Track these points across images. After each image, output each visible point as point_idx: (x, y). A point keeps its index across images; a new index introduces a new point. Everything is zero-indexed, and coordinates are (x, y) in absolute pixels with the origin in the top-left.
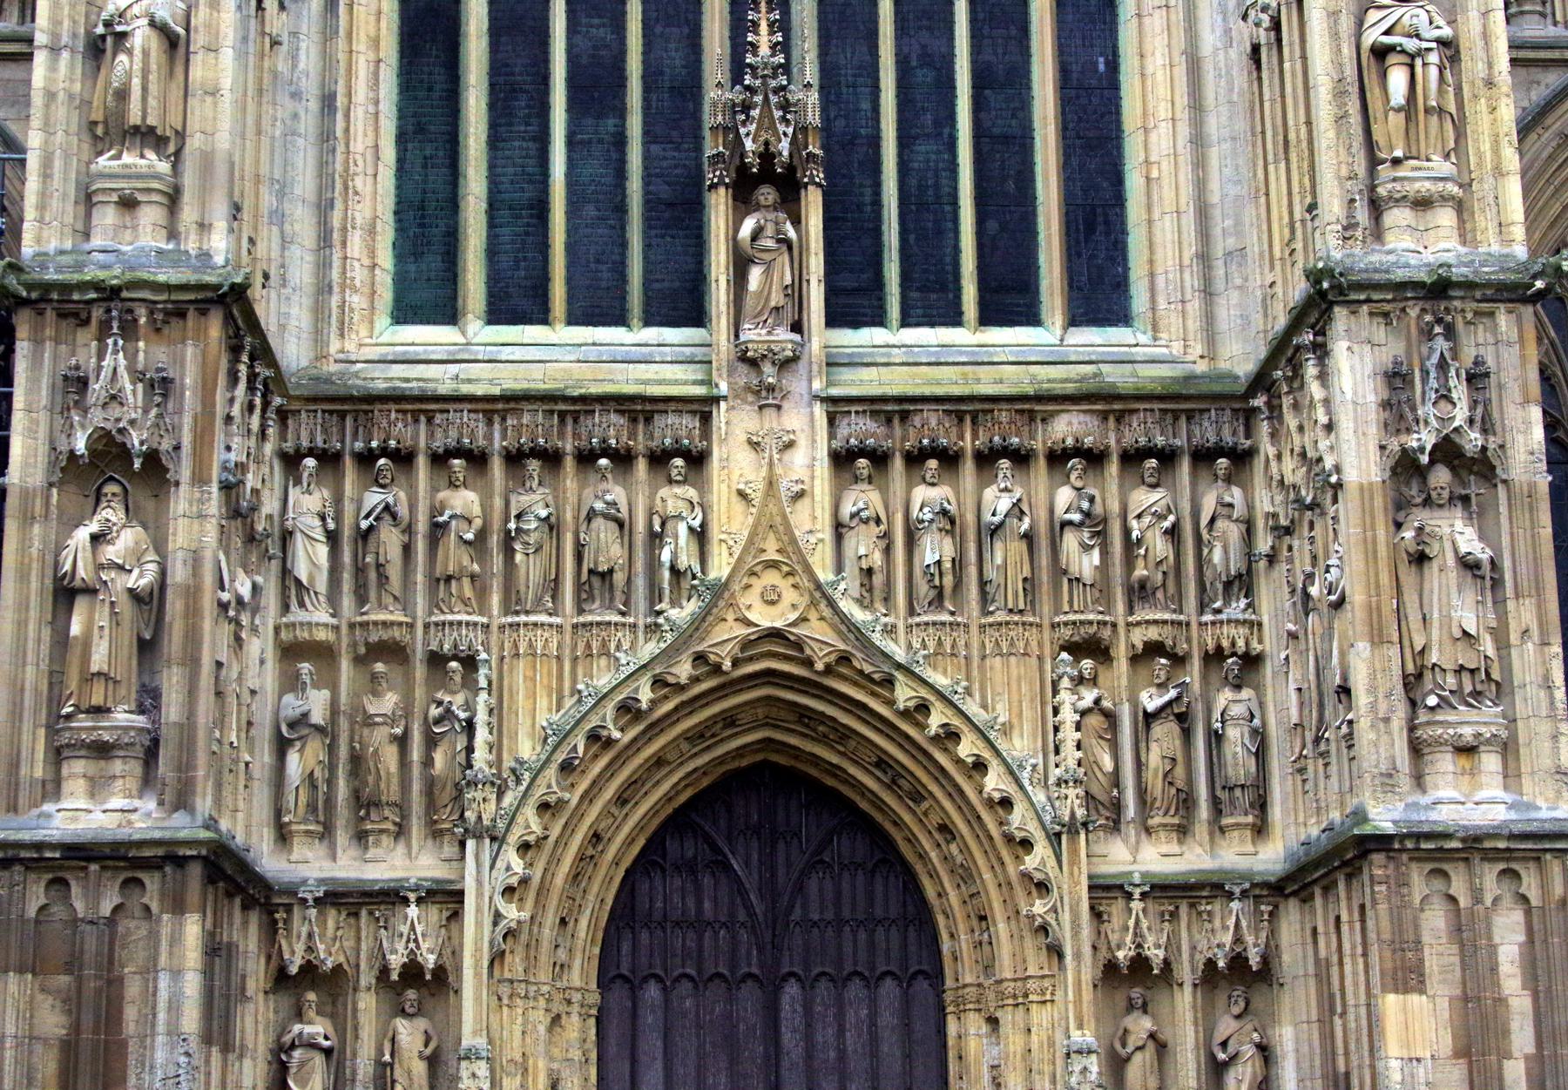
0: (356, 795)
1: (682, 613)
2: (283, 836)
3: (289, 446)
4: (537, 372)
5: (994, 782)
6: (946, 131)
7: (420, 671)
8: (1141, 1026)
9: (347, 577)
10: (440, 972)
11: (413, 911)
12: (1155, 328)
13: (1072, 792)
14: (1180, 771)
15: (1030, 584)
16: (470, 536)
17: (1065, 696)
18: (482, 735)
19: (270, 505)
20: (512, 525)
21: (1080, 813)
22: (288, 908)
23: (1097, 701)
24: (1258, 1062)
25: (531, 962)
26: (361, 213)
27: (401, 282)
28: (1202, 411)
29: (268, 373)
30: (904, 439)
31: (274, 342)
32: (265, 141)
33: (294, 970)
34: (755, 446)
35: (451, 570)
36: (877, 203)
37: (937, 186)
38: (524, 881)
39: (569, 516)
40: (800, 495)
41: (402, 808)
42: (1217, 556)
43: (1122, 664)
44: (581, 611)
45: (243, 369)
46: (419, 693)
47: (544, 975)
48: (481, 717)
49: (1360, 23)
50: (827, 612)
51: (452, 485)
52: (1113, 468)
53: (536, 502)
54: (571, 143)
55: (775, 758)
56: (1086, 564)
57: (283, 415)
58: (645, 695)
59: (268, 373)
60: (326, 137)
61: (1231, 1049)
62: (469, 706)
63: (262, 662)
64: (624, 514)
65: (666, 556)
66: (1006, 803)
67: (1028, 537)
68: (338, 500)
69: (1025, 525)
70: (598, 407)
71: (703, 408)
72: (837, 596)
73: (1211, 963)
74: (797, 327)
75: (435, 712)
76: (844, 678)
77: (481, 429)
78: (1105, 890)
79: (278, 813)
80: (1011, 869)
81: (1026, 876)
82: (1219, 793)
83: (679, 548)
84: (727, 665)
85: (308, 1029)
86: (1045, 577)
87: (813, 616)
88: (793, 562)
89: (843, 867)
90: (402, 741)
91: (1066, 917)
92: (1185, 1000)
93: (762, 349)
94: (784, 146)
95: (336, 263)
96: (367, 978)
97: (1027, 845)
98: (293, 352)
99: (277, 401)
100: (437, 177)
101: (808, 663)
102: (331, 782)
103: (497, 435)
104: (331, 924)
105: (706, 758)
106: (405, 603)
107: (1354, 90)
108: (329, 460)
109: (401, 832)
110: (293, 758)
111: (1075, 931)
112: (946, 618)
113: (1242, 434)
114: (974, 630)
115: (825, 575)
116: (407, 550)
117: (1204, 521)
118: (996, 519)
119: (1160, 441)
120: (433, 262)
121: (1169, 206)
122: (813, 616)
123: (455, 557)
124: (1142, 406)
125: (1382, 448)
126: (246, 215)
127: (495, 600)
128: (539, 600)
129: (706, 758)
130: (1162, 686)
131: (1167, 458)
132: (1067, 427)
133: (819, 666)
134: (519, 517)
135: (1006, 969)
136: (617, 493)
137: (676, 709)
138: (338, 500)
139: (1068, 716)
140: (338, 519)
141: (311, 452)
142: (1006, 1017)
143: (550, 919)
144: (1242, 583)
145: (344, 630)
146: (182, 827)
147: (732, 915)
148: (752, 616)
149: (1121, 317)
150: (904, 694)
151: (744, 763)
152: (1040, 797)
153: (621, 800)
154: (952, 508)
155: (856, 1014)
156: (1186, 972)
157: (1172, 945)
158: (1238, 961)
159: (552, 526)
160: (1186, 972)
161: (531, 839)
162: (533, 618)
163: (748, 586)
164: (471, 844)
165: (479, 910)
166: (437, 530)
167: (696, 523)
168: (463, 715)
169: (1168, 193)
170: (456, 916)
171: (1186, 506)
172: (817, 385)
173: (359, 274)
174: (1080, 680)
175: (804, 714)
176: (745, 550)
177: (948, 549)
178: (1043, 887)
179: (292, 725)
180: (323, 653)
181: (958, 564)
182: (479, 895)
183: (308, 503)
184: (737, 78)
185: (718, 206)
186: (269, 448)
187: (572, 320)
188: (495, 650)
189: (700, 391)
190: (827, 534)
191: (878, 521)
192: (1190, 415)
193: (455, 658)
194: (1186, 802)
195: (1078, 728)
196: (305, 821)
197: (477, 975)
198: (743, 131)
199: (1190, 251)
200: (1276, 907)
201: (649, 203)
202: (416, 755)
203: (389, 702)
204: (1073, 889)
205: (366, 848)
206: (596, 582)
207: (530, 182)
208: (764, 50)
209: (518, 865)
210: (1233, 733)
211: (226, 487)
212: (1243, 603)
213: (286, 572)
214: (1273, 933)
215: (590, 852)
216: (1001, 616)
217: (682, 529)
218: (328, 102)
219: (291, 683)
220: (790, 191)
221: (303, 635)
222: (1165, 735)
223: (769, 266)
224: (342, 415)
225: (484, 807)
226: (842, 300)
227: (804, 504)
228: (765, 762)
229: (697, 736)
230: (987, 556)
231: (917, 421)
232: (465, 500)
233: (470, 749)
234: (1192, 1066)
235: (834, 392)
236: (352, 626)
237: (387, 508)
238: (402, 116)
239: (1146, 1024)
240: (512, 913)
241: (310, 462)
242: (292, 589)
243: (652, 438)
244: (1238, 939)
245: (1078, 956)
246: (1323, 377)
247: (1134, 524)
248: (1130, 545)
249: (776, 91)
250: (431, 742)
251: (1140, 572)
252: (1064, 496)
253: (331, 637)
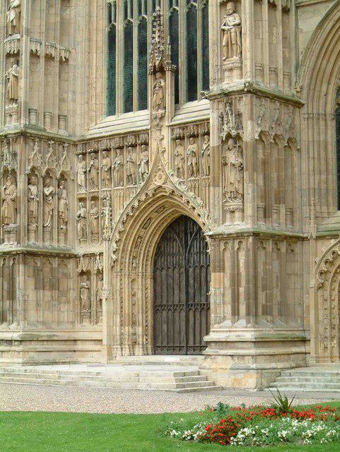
163: (155, 176)
240: (114, 257)
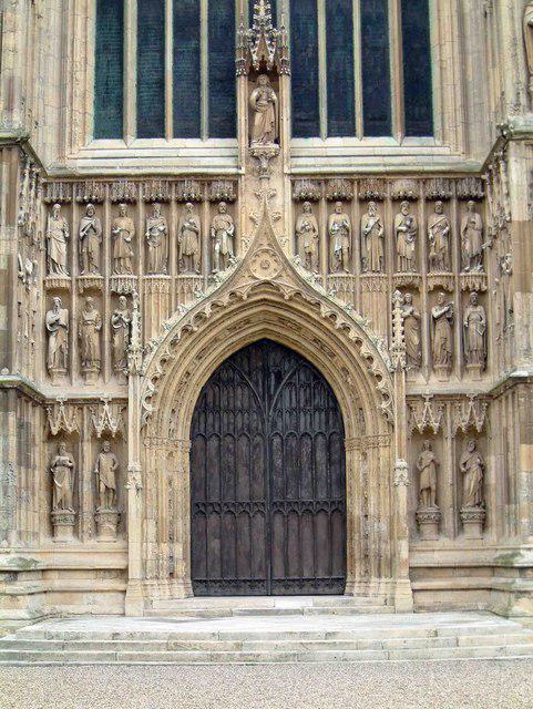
0: (81, 357)
1: (224, 275)
2: (49, 373)
3: (48, 199)
4: (160, 162)
5: (365, 350)
6: (333, 68)
7: (108, 300)
8: (428, 456)
9: (75, 258)
10: (119, 434)
11: (106, 407)
12: (443, 138)
13: (399, 354)
14: (448, 344)
15: (383, 259)
16: (129, 239)
17: (397, 311)
18: (135, 330)
19: (40, 227)
20: (148, 234)
21: (403, 363)
22: (53, 406)
23: (411, 313)
24: (479, 471)
25: (159, 430)
26: (79, 90)
27: (98, 119)
28: (462, 179)
29: (38, 170)
30: (327, 192)
31: (39, 156)
32: (36, 62)
33: (55, 432)
34: (258, 196)
35: (120, 255)
36: (316, 79)
37: (344, 71)
38: (155, 394)
39: (174, 229)
40: (278, 219)
41: (102, 362)
42: (468, 246)
43: (424, 295)
44: (179, 273)
45: (27, 172)
46: (107, 310)
47: (165, 434)
48: (134, 323)
49: (524, 11)
50: (290, 272)
51: (121, 216)
52: (422, 205)
53: (158, 223)
54: (176, 53)
55: (268, 337)
56: (407, 248)
57: (45, 185)
58: (208, 311)
59: (38, 170)
60: (63, 57)
61: (467, 467)
62: (129, 316)
63: (38, 297)
64: (198, 228)
65: (217, 247)
66: (370, 359)
67: (383, 238)
68: (70, 222)
69: (381, 232)
70: (186, 179)
71: (234, 180)
72: (294, 265)
73: (460, 429)
74: (277, 141)
75: (114, 319)
76: (297, 302)
77: (134, 190)
78: (412, 400)
79: (47, 364)
80: (372, 388)
81: (378, 391)
82: (466, 353)
83: (224, 244)
84: (245, 297)
85: (62, 458)
86: (390, 255)
87: (284, 275)
88: (274, 249)
89: (302, 386)
90: (101, 332)
91: (395, 409)
92: (447, 448)
93: (261, 152)
94: (271, 57)
95: (68, 113)
96: (87, 436)
97: (379, 377)
98: (49, 158)
99: (43, 180)
100: (114, 72)
101: (282, 296)
102: (69, 350)
103: (141, 192)
104: (71, 412)
105: (238, 337)
106: (101, 271)
107: (520, 43)
108: (65, 204)
109: (101, 371)
110: (52, 339)
111: (399, 417)
112: (344, 275)
113: (480, 189)
114: (358, 280)
115: (289, 255)
116: (101, 245)
117: (462, 230)
118: (368, 229)
119: (443, 193)
120: (112, 111)
121: (450, 82)
122: (284, 275)
123: (123, 248)
124: (434, 177)
125: (529, 205)
126: (28, 100)
127: (141, 268)
128: (160, 268)
129: (238, 337)
130: (442, 305)
131: (446, 200)
132: (401, 186)
133: (287, 297)
134: (151, 230)
135: (370, 430)
136: (195, 219)
137: (223, 316)
138: (70, 222)
139: (399, 320)
140: (70, 231)
141: (57, 202)
142: (370, 453)
143: (167, 410)
144: (479, 258)
145: (74, 282)
147: (250, 406)
148: (256, 275)
149: (429, 132)
150: (325, 311)
151: (256, 339)
152: (385, 355)
153: (199, 357)
154: (348, 225)
155: (306, 450)
156: (448, 433)
157: (443, 421)
158: (471, 429)
159: (166, 234)
160: (448, 433)
161: (158, 375)
162: (157, 276)
164: (130, 377)
165: (135, 407)
166: (114, 237)
167: (231, 232)
168: (127, 320)
169: (449, 74)
170: (125, 409)
171: (454, 222)
172: (286, 171)
173: (78, 117)
174: (405, 303)
175: (282, 319)
176: (254, 244)
177: (346, 244)
178: (386, 396)
179: (51, 325)
180: (65, 293)
181: (351, 250)
182: (135, 400)
183: (57, 225)
184: (251, 22)
185: (242, 85)
186: (39, 202)
187: (176, 136)
188: (141, 290)
189: (234, 171)
190: (291, 237)
191: (314, 231)
192: (457, 181)
193: (123, 294)
194: (451, 358)
195: (403, 325)
196: (59, 367)
197: (135, 435)
198: (252, 51)
199: (459, 103)
200: (489, 404)
201: (212, 80)
202: (107, 337)
203: (94, 314)
204: (398, 395)
205: (85, 379)
206: (186, 260)
207: (157, 72)
208: (262, 13)
209: (152, 387)
210: (472, 327)
211: (21, 226)
212: (479, 267)
213: (47, 256)
214: (488, 415)
215: (185, 380)
216: (369, 274)
217: (225, 235)
218: (63, 38)
219: (52, 307)
220: (274, 76)
221: (55, 285)
222: (442, 326)
223: (264, 113)
224: (71, 184)
225: (135, 361)
226: (301, 124)
227: (279, 223)
228: (265, 339)
229: (231, 329)
230: (363, 246)
231: (332, 184)
232: (125, 223)
233: (130, 336)
234: (450, 472)
235: (294, 171)
236: (77, 280)
237: (92, 227)
238: (97, 43)
239: (431, 456)
241: (57, 206)
242: (50, 264)
243: (211, 193)
244: (471, 419)
245: (400, 427)
246: (506, 170)
247: (430, 231)
248: (428, 241)
249: (267, 32)
250: (113, 332)
251: (432, 253)
252: (399, 218)
253: (68, 285)
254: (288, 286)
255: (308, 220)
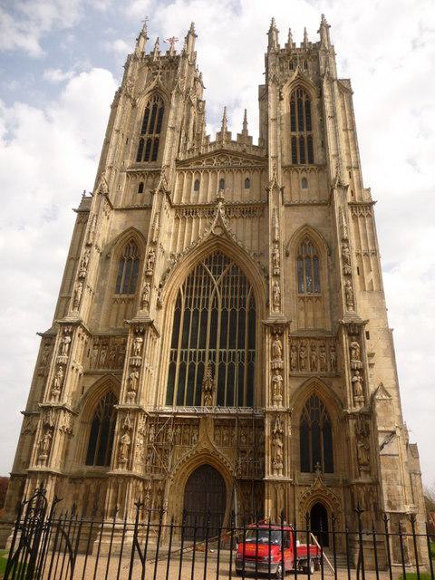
60: (158, 384)
83: (195, 438)
146: (130, 473)
150: (221, 457)
254: (211, 450)
255: (218, 432)
